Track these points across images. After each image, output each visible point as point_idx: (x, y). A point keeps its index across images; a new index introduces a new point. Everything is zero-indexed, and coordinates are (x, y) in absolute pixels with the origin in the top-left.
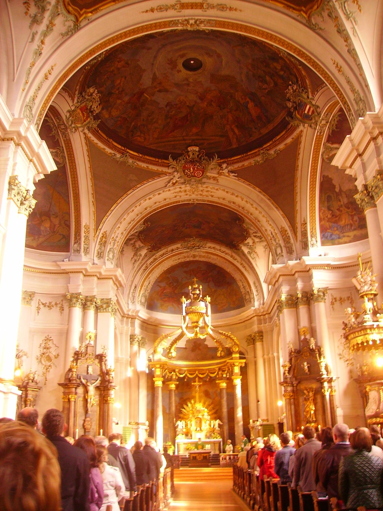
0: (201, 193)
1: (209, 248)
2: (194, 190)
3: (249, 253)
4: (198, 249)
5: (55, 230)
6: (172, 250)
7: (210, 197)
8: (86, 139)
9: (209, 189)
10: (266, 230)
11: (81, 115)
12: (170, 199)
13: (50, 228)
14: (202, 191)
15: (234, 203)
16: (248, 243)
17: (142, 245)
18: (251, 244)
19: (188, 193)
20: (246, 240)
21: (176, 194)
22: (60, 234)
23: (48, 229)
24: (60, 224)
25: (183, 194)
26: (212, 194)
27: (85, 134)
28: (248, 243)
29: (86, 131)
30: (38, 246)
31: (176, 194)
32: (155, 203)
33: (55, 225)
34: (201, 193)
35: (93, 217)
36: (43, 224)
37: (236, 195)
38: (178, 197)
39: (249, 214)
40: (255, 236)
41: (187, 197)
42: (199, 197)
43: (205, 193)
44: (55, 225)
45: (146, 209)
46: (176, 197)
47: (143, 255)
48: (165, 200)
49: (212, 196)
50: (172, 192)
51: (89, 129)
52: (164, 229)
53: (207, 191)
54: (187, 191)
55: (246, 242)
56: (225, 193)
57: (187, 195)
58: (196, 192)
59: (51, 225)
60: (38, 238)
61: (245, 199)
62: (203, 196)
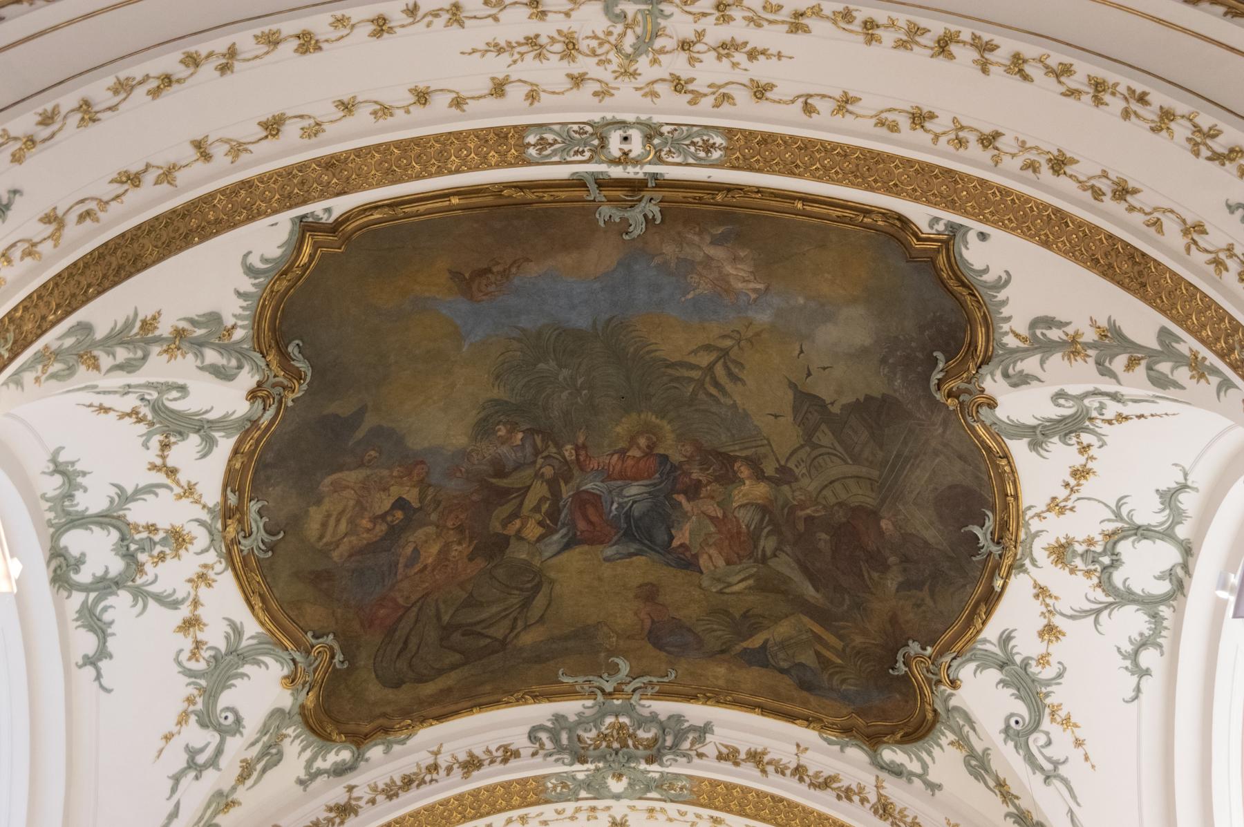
0: (677, 64)
1: (720, 757)
2: (629, 41)
3: (1017, 734)
4: (650, 760)
6: (471, 764)
7: (742, 97)
9: (737, 30)
10: (1193, 230)
12: (458, 102)
14: (685, 45)
15: (919, 118)
16: (1006, 639)
17: (252, 627)
18: (1027, 646)
19: (584, 64)
20: (991, 599)
21: (498, 66)
25: (552, 72)
26: (761, 70)
28: (1006, 639)
31: (498, 66)
32: (347, 107)
34: (677, 64)
37: (937, 27)
38: (516, 94)
39: (1046, 172)
40: (1062, 552)
41: (580, 110)
42: (671, 111)
43: (710, 70)
45: (273, 127)
46: (499, 89)
47: (253, 722)
48: (422, 97)
49: (760, 91)
50: (479, 33)
52: (412, 495)
53: (726, 48)
54: (583, 45)
55: (991, 632)
56: (854, 43)
57: (578, 80)
58: (643, 63)
61: (1007, 46)
62: (696, 97)
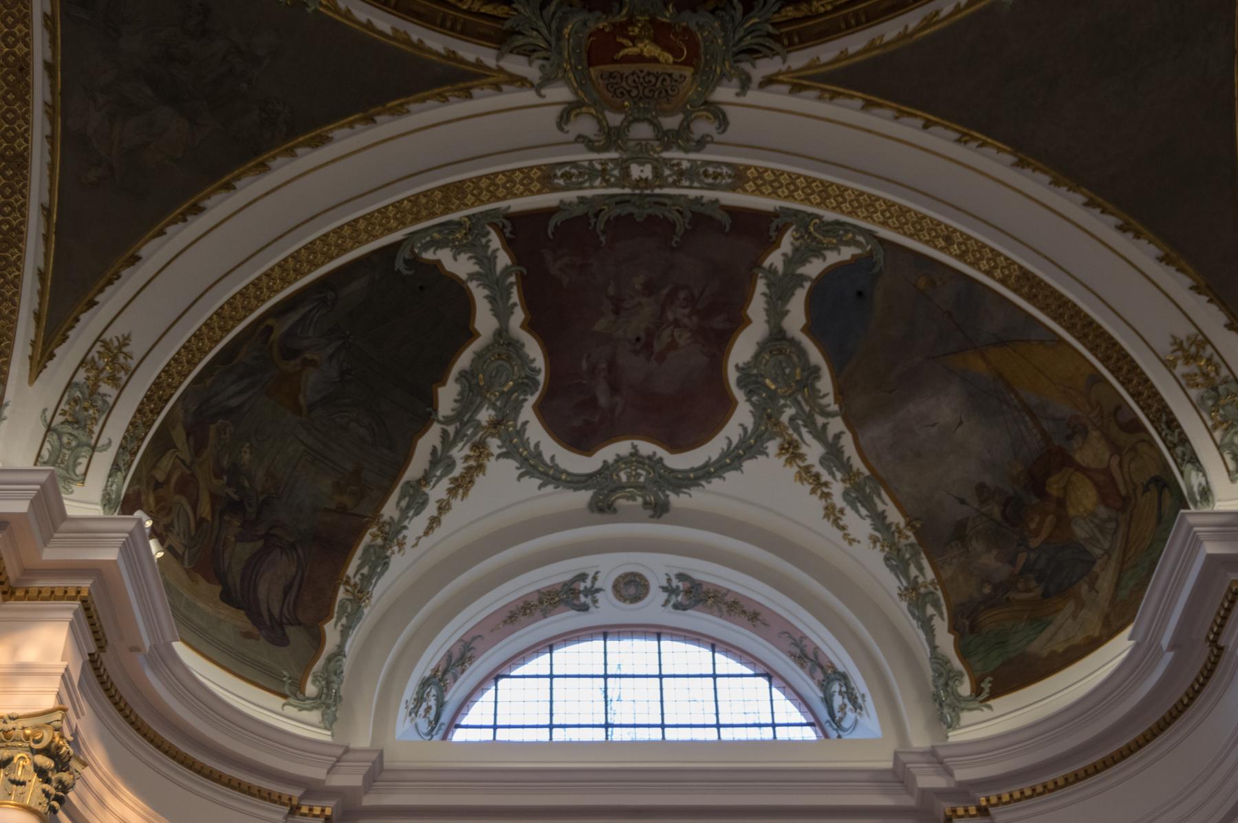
5: (1123, 492)
8: (806, 88)
11: (627, 69)
13: (1103, 499)
22: (1146, 489)
23: (1103, 512)
24: (1116, 448)
27: (768, 82)
29: (766, 67)
30: (1107, 622)
33: (1107, 471)
35: (1177, 283)
36: (1072, 512)
44: (1107, 471)
51: (753, 53)
59: (1096, 484)
60: (1092, 587)
